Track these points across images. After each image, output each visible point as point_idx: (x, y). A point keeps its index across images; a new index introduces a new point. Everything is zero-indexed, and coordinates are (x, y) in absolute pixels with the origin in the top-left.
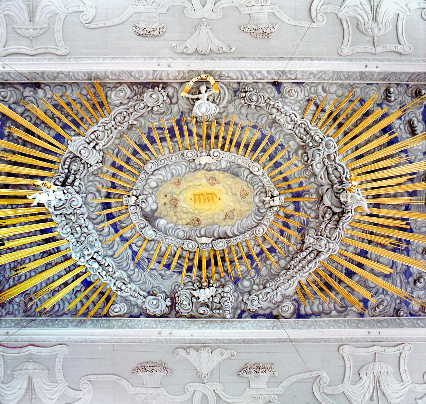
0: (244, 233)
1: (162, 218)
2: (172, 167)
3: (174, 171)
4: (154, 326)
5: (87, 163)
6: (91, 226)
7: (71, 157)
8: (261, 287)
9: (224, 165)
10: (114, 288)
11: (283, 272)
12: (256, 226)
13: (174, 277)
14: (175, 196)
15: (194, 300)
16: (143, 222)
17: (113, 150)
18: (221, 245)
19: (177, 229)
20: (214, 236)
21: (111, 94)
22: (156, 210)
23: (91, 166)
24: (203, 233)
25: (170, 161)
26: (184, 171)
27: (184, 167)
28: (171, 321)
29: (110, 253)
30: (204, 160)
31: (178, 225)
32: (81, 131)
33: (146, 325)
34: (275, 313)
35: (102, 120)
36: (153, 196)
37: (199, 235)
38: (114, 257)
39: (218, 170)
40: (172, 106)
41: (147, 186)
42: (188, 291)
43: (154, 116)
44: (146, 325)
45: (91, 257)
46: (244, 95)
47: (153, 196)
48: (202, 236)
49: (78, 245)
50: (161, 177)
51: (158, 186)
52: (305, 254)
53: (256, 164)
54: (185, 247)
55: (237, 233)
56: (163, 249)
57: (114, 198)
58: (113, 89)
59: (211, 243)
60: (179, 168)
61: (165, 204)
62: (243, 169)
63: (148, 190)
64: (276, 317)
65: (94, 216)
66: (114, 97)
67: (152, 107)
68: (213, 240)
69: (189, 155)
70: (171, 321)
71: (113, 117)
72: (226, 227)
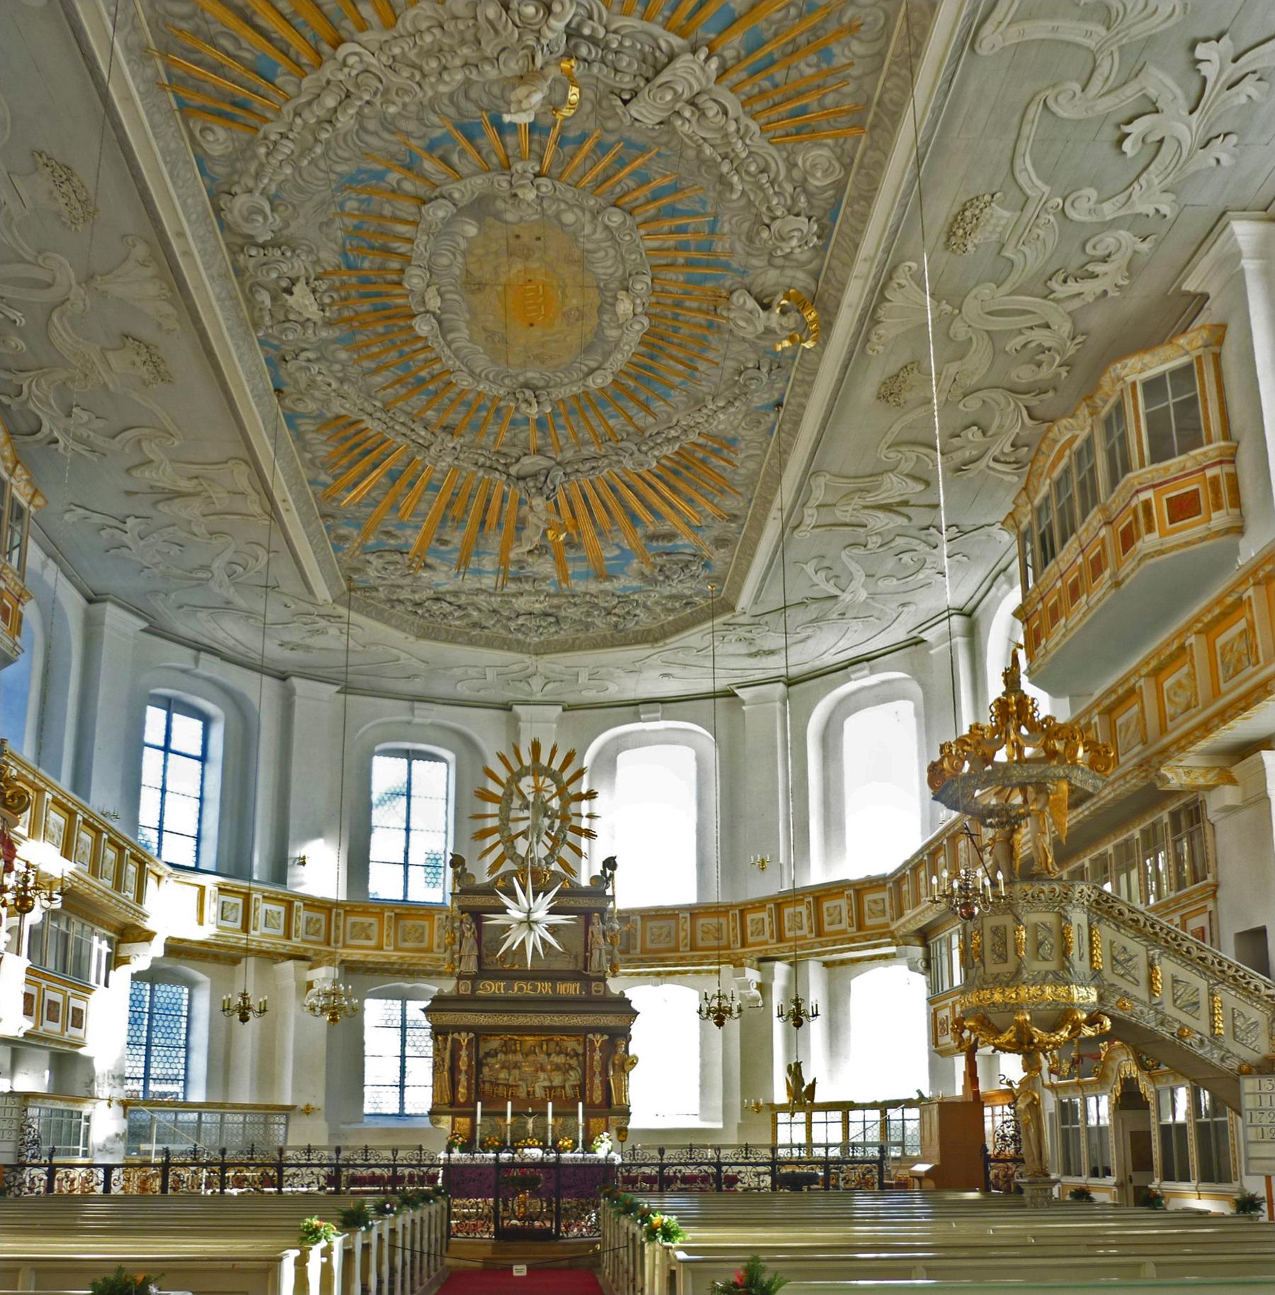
0: (457, 357)
1: (479, 230)
2: (612, 252)
3: (601, 254)
4: (194, 216)
5: (635, 94)
6: (442, 89)
7: (658, 54)
8: (340, 375)
9: (612, 333)
10: (273, 130)
11: (378, 404)
12: (472, 373)
13: (332, 245)
15: (284, 284)
17: (666, 145)
18: (423, 327)
19: (454, 254)
20: (443, 313)
22: (501, 220)
23: (625, 102)
24: (448, 296)
26: (600, 271)
27: (610, 271)
29: (371, 125)
30: (624, 307)
31: (464, 257)
32: (734, 77)
34: (285, 389)
35: (754, 126)
36: (536, 217)
37: (443, 289)
38: (361, 132)
39: (600, 324)
40: (766, 257)
41: (563, 206)
42: (303, 272)
43: (746, 226)
44: (190, 201)
45: (352, 90)
46: (764, 370)
47: (536, 217)
48: (440, 294)
49: (384, 59)
50: (588, 230)
52: (423, 433)
53: (610, 379)
54: (412, 271)
55: (454, 346)
56: (401, 229)
57: (530, 142)
58: (839, 150)
59: (427, 312)
60: (610, 263)
61: (518, 237)
62: (600, 359)
63: (554, 207)
64: (278, 391)
65: (474, 94)
66: (817, 160)
67: (768, 226)
68: (434, 314)
69: (638, 286)
70: (217, 239)
71: (760, 151)
72: (467, 332)
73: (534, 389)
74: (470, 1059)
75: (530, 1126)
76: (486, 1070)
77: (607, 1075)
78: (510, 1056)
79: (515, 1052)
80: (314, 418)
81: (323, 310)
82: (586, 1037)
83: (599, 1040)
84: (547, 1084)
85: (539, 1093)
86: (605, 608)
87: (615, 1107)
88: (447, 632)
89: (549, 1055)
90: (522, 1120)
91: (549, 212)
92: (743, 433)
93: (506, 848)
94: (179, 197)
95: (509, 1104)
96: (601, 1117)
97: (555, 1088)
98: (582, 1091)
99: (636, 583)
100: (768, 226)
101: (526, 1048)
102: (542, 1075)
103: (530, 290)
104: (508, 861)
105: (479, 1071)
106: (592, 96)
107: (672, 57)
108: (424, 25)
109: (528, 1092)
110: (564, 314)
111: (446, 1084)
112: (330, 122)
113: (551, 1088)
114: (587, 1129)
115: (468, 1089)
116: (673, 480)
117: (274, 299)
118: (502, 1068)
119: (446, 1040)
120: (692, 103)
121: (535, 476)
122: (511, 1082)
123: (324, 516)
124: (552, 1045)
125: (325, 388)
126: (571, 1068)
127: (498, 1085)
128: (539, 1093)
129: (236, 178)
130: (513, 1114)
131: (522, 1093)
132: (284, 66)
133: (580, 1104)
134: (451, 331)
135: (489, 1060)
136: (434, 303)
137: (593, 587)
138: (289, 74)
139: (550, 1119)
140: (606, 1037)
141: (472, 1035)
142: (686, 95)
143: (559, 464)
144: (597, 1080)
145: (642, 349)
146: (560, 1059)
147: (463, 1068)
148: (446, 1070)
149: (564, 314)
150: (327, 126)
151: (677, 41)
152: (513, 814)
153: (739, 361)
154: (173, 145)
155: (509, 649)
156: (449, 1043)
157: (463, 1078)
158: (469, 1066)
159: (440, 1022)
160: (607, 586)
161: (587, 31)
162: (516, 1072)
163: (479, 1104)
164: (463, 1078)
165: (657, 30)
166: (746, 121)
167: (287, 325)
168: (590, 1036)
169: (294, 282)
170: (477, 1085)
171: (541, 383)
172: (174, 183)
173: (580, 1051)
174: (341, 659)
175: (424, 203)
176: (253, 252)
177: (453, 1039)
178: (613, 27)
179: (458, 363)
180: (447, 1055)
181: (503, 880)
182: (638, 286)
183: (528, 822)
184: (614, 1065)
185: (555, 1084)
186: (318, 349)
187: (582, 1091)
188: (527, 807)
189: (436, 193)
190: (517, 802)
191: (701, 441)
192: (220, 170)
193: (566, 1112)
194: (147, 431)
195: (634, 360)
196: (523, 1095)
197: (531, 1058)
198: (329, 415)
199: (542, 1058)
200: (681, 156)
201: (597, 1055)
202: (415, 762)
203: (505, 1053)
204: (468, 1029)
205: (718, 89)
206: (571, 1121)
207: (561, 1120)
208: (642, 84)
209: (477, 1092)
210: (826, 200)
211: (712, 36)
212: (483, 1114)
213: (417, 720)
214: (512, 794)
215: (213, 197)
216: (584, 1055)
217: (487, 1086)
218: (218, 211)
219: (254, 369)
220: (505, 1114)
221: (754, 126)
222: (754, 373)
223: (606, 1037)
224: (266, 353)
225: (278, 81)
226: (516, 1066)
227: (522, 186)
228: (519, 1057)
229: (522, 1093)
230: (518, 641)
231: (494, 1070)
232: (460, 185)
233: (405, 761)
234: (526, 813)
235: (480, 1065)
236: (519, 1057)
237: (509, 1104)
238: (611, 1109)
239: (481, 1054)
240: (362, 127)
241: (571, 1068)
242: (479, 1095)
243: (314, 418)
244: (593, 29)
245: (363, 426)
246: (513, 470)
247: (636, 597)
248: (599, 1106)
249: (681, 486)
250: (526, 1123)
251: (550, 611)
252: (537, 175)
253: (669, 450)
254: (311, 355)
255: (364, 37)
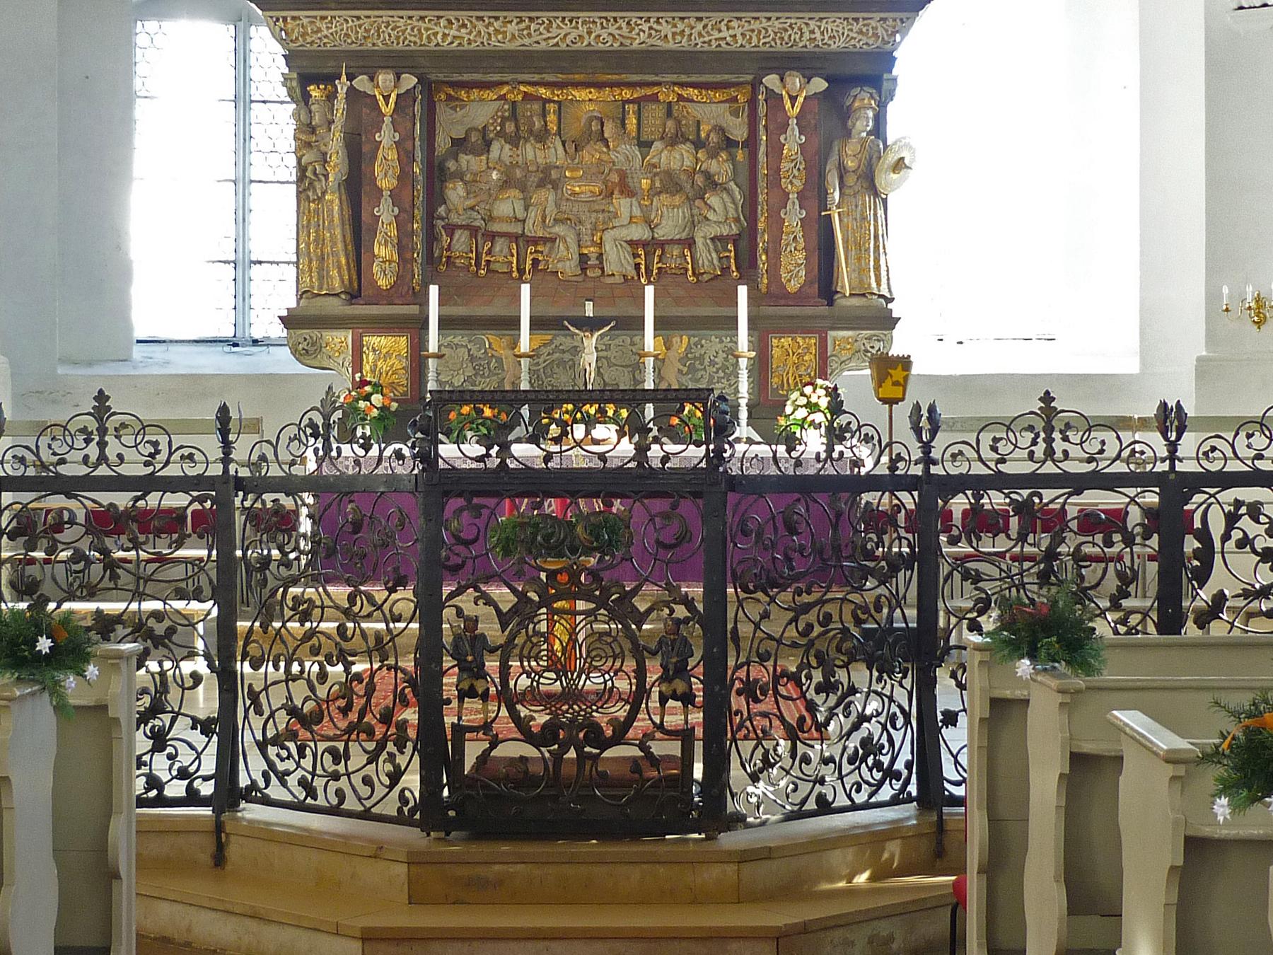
74: (406, 158)
75: (589, 358)
76: (456, 193)
77: (823, 195)
78: (530, 151)
79: (542, 137)
82: (756, 84)
83: (798, 90)
84: (639, 232)
85: (617, 261)
87: (845, 302)
89: (644, 145)
90: (563, 341)
95: (525, 289)
96: (806, 331)
97: (662, 244)
98: (744, 252)
101: (573, 130)
102: (623, 206)
105: (435, 196)
109: (583, 258)
111: (336, 233)
113: (651, 246)
114: (761, 367)
115: (402, 247)
118: (506, 184)
119: (331, 97)
122: (532, 229)
124: (654, 114)
126: (712, 183)
127: (492, 236)
128: (617, 261)
130: (536, 324)
131: (564, 260)
133: (743, 291)
135: (464, 158)
139: (650, 340)
140: (819, 85)
141: (409, 81)
144: (793, 216)
146: (680, 158)
147: (386, 182)
148: (339, 188)
156: (340, 104)
157: (385, 213)
158: (404, 176)
159: (312, 43)
162: (546, 197)
163: (434, 290)
164: (385, 213)
168: (771, 80)
170: (431, 237)
173: (739, 131)
177: (352, 93)
180: (335, 144)
184: (842, 172)
185: (661, 234)
187: (744, 252)
193: (695, 315)
196: (569, 267)
197: (591, 154)
199: (624, 153)
201: (793, 141)
203: (515, 141)
204: (398, 62)
206: (712, 345)
207: (682, 342)
209: (430, 255)
212: (444, 323)
216: (751, 144)
217: (461, 237)
220: (515, 323)
223: (819, 85)
226: (548, 178)
228: (555, 153)
229: (564, 260)
231: (484, 192)
235: (437, 175)
236: (555, 153)
237: (525, 289)
238: (832, 300)
239: (442, 143)
241: (712, 183)
242: (435, 265)
248: (799, 298)
250: (577, 351)
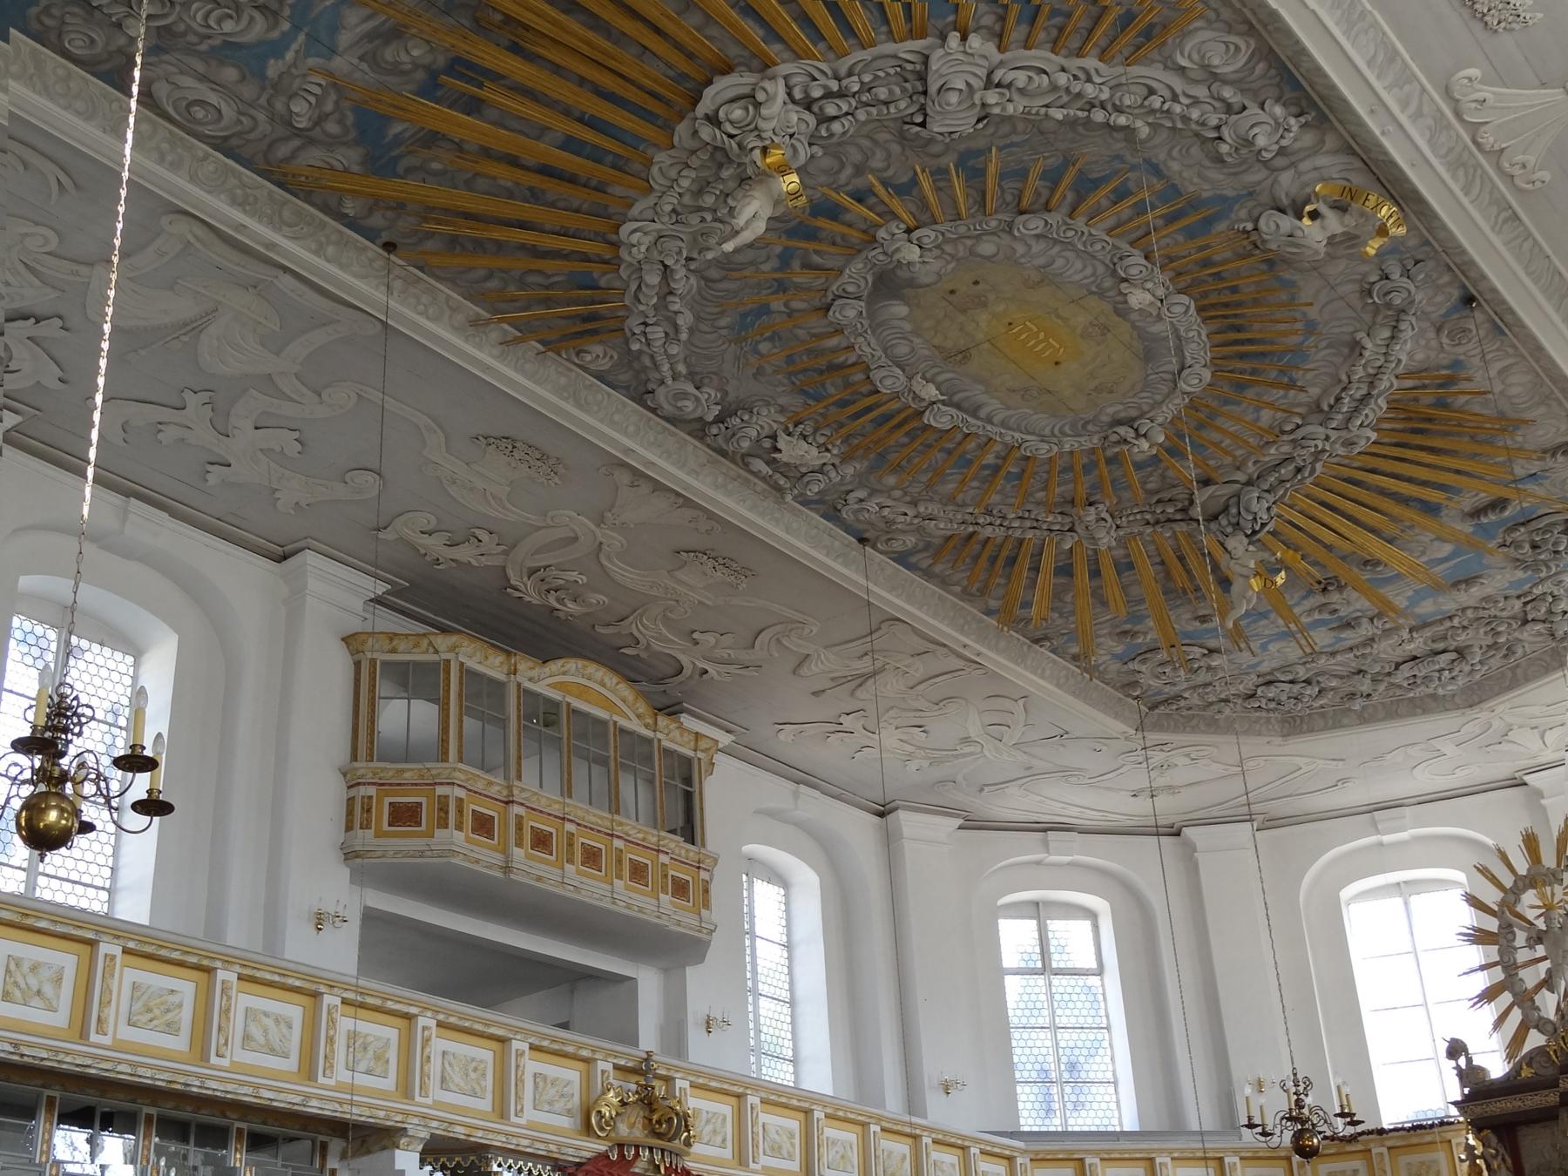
1: (909, 305)
2: (1068, 254)
3: (1060, 262)
4: (631, 429)
14: (991, 297)
15: (767, 444)
16: (863, 284)
18: (941, 419)
21: (1197, 29)
24: (940, 378)
25: (1084, 244)
26: (1077, 277)
27: (1089, 271)
28: (673, 434)
31: (919, 336)
33: (617, 418)
41: (969, 242)
44: (617, 418)
51: (988, 258)
56: (833, 342)
60: (1079, 265)
61: (952, 292)
73: (1129, 422)
80: (926, 549)
81: (827, 450)
86: (1513, 618)
88: (1323, 715)
91: (961, 254)
92: (1460, 350)
93: (1525, 1016)
94: (601, 421)
99: (1520, 574)
100: (1220, 138)
103: (1020, 333)
104: (1533, 1033)
106: (887, 136)
107: (926, 59)
108: (673, 173)
110: (1082, 336)
112: (671, 293)
116: (1417, 440)
117: (771, 462)
120: (989, 84)
121: (1226, 509)
123: (1036, 641)
125: (902, 518)
129: (643, 377)
132: (596, 269)
134: (979, 407)
136: (930, 392)
137: (1449, 603)
138: (605, 273)
142: (977, 84)
143: (1249, 483)
145: (1215, 325)
149: (1082, 336)
150: (670, 298)
151: (918, 44)
152: (1523, 956)
153: (1354, 281)
154: (563, 381)
155: (1425, 711)
160: (1476, 591)
161: (817, 93)
165: (889, 48)
166: (1074, 64)
167: (806, 479)
169: (774, 437)
171: (1134, 413)
172: (586, 411)
174: (1236, 787)
175: (828, 310)
176: (714, 431)
178: (843, 71)
179: (1017, 435)
181: (1529, 1065)
182: (1134, 271)
183: (1547, 964)
186: (861, 485)
188: (1540, 940)
189: (831, 297)
190: (1521, 938)
191: (1409, 383)
192: (624, 377)
194: (778, 628)
195: (1220, 338)
198: (937, 541)
200: (1042, 133)
202: (1414, 899)
205: (1008, 55)
208: (922, 100)
210: (1263, 76)
211: (951, 18)
213: (1386, 839)
214: (1510, 926)
215: (640, 401)
218: (653, 411)
219: (814, 532)
221: (1091, 63)
222: (1388, 285)
224: (816, 511)
225: (602, 283)
227: (898, 250)
230: (1434, 696)
232: (845, 278)
233: (1399, 901)
234: (1540, 951)
240: (707, 280)
243: (926, 549)
244: (825, 87)
245: (982, 537)
246: (1197, 512)
247: (1537, 591)
249: (1437, 443)
251: (1441, 646)
252: (909, 231)
253: (1371, 413)
254: (861, 494)
255: (634, 212)
